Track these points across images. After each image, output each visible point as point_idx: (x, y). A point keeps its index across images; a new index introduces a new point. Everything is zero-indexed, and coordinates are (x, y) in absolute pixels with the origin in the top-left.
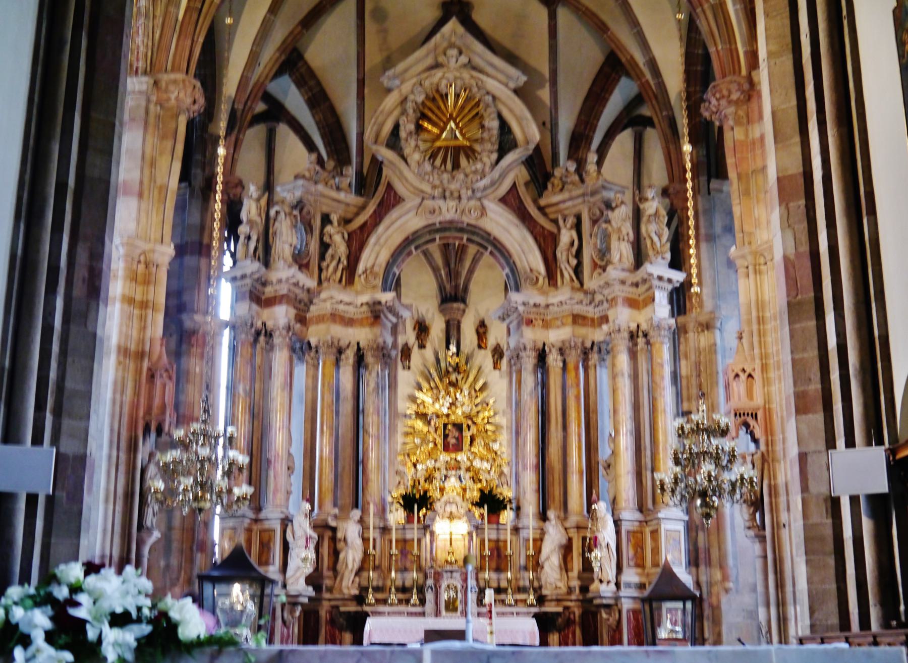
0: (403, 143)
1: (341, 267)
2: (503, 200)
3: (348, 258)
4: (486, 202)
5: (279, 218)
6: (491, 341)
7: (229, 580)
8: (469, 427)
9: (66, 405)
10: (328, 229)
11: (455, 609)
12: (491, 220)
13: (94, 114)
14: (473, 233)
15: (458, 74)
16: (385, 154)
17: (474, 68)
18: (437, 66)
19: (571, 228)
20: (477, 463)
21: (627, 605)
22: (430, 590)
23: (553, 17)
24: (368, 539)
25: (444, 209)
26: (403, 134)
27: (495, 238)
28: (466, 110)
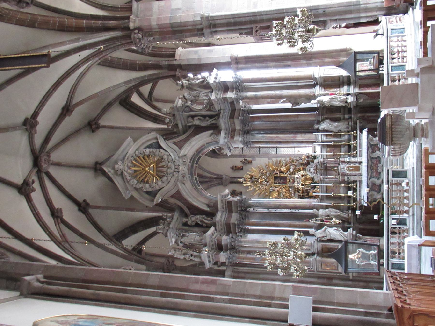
0: (154, 190)
1: (206, 218)
2: (180, 148)
3: (202, 215)
4: (181, 154)
5: (184, 242)
8: (276, 174)
9: (269, 295)
10: (189, 223)
11: (359, 167)
12: (188, 153)
13: (129, 282)
14: (194, 161)
15: (126, 165)
17: (124, 159)
19: (193, 119)
20: (291, 170)
21: (357, 91)
22: (349, 178)
23: (104, 127)
24: (326, 205)
25: (183, 172)
26: (150, 190)
27: (196, 152)
28: (142, 163)
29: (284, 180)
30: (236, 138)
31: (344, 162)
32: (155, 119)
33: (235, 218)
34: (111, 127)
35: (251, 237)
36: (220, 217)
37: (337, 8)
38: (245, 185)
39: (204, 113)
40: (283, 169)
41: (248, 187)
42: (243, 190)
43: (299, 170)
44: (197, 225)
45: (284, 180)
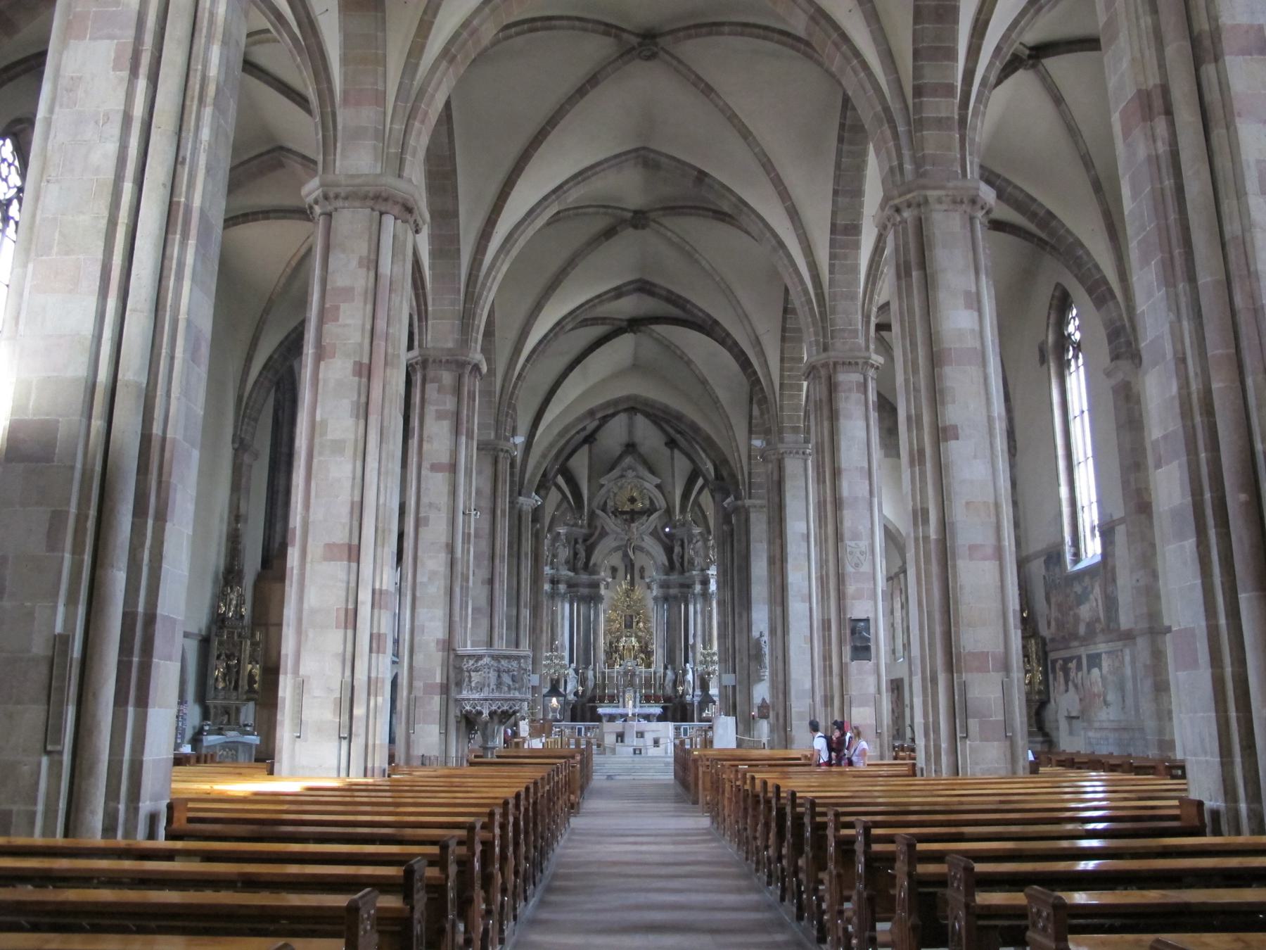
2: (651, 534)
6: (647, 574)
10: (578, 546)
16: (599, 512)
18: (622, 476)
20: (640, 634)
21: (696, 704)
29: (629, 625)
30: (661, 590)
31: (635, 692)
32: (686, 496)
33: (584, 591)
34: (672, 459)
35: (567, 606)
36: (584, 577)
37: (817, 681)
40: (641, 625)
41: (621, 585)
42: (617, 580)
43: (639, 642)
44: (576, 554)
45: (629, 625)
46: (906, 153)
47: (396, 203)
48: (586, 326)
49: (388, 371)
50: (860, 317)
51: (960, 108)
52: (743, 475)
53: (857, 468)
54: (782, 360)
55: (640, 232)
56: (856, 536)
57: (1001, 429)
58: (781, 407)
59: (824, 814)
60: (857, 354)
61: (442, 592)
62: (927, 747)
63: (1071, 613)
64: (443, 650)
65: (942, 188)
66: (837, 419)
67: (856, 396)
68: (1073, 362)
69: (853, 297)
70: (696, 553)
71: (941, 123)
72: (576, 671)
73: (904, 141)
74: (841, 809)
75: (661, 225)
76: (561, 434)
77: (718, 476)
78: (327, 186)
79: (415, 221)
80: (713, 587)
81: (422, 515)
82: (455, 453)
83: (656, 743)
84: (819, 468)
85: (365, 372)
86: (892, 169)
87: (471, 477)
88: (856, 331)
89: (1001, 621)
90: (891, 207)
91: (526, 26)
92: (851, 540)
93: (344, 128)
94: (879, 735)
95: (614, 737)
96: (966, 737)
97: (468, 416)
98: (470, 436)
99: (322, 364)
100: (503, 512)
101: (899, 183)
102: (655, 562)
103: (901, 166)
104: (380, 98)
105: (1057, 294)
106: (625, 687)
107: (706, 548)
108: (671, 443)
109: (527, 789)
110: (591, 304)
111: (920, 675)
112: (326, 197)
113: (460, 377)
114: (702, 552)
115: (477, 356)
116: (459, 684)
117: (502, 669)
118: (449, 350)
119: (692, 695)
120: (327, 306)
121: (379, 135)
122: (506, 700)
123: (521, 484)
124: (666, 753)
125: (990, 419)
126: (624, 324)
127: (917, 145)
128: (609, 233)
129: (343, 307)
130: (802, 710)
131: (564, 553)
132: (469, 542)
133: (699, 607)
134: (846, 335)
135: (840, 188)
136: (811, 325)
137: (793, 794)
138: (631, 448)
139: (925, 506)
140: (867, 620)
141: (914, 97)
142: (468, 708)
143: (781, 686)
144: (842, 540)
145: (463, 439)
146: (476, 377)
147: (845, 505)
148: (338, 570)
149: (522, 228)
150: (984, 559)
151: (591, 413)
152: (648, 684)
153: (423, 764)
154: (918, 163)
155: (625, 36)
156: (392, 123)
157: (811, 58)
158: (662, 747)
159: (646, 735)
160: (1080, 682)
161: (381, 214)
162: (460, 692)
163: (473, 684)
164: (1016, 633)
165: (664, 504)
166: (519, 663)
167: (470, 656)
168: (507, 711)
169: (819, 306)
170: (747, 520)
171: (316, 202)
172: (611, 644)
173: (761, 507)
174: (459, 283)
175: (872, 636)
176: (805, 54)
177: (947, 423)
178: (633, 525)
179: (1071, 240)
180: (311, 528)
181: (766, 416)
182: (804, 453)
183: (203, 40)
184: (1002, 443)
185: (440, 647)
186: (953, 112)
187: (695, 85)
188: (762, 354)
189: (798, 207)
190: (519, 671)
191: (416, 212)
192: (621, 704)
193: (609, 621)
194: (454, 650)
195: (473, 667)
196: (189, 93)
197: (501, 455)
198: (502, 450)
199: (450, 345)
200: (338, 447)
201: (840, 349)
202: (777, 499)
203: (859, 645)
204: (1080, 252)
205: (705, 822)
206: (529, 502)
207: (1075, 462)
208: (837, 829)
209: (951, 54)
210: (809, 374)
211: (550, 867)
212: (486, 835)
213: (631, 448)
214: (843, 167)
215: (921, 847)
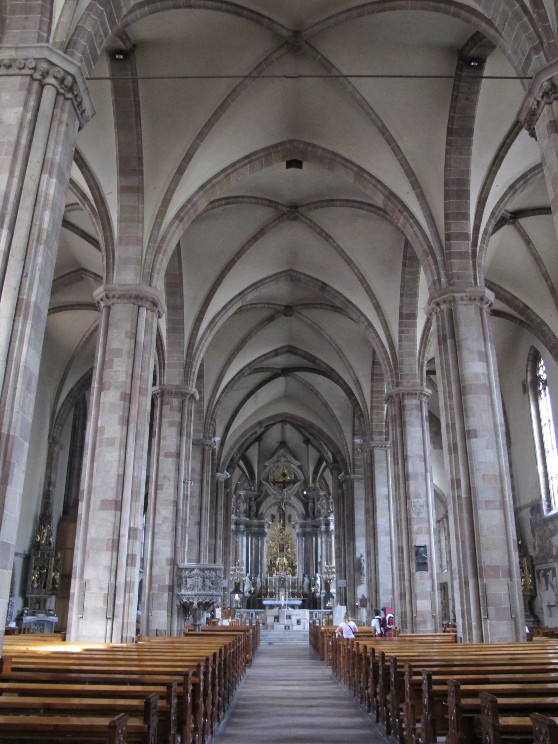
2: (295, 495)
6: (293, 519)
7: (235, 593)
10: (252, 502)
20: (288, 555)
21: (322, 598)
30: (301, 529)
31: (286, 591)
32: (316, 472)
33: (255, 529)
35: (245, 539)
36: (255, 521)
37: (395, 584)
38: (278, 525)
39: (316, 509)
40: (289, 550)
41: (277, 526)
43: (288, 560)
46: (442, 272)
47: (147, 300)
48: (258, 372)
49: (141, 398)
50: (417, 367)
51: (472, 246)
52: (349, 460)
53: (417, 455)
54: (372, 392)
55: (289, 318)
56: (418, 496)
57: (502, 432)
58: (372, 419)
59: (402, 667)
60: (416, 388)
61: (170, 529)
62: (463, 625)
63: (548, 541)
64: (171, 565)
65: (463, 291)
66: (405, 427)
67: (416, 413)
68: (542, 392)
69: (413, 355)
70: (322, 507)
71: (462, 255)
72: (250, 578)
73: (440, 265)
74: (413, 664)
75: (301, 314)
76: (242, 436)
77: (335, 461)
78: (108, 291)
79: (158, 311)
80: (332, 527)
81: (159, 483)
82: (179, 446)
83: (298, 622)
84: (395, 455)
85: (128, 399)
86: (434, 281)
87: (189, 461)
88: (415, 375)
89: (506, 547)
90: (434, 303)
91: (224, 202)
92: (415, 498)
93: (119, 257)
94: (434, 617)
95: (273, 619)
96: (487, 619)
97: (187, 425)
98: (188, 436)
99: (103, 393)
100: (207, 481)
101: (438, 289)
102: (297, 512)
103: (439, 279)
104: (140, 241)
105: (532, 352)
106: (280, 588)
107: (328, 503)
108: (307, 441)
109: (220, 650)
110: (260, 360)
111: (458, 580)
112: (107, 297)
113: (183, 402)
114: (325, 507)
115: (193, 390)
116: (180, 586)
117: (206, 576)
118: (177, 386)
119: (321, 593)
120: (106, 359)
121: (139, 262)
122: (208, 595)
123: (218, 465)
124: (305, 628)
125: (495, 425)
126: (279, 371)
127: (447, 267)
128: (271, 319)
129: (115, 360)
130: (387, 601)
131: (243, 507)
132: (187, 500)
133: (324, 539)
134: (409, 377)
135: (405, 292)
136: (388, 371)
137: (383, 654)
138: (283, 444)
139: (458, 477)
140: (425, 547)
141: (446, 240)
142: (185, 600)
143: (374, 587)
144: (409, 498)
145: (184, 438)
146: (192, 402)
147: (411, 478)
148: (109, 515)
149: (220, 315)
150: (495, 509)
151: (260, 423)
152: (293, 586)
153: (157, 635)
154: (449, 277)
155: (280, 206)
156: (146, 255)
157: (386, 219)
158: (302, 625)
159: (293, 617)
160: (555, 584)
161: (139, 307)
162: (180, 591)
163: (188, 586)
164: (515, 555)
165: (302, 477)
166: (216, 573)
167: (186, 569)
168: (208, 602)
169: (393, 360)
170: (352, 487)
171: (102, 300)
172: (271, 561)
173: (360, 479)
174: (183, 347)
175: (428, 557)
176: (382, 216)
177: (470, 428)
178: (284, 490)
179: (538, 321)
180: (93, 490)
181: (363, 425)
182: (385, 447)
183: (41, 208)
184: (502, 439)
185: (169, 563)
186: (468, 249)
187: (319, 233)
188: (360, 388)
189: (380, 303)
190: (216, 578)
191: (159, 306)
192: (277, 598)
193: (270, 547)
194: (177, 565)
195: (188, 576)
196: (31, 237)
197: (207, 448)
198: (207, 445)
199: (178, 383)
200: (110, 442)
201: (406, 386)
202: (369, 474)
203: (420, 561)
204: (545, 328)
205: (329, 671)
206: (223, 476)
207: (546, 451)
208: (410, 676)
209: (466, 216)
210: (388, 400)
211: (234, 701)
212: (195, 679)
213: (283, 444)
214: (405, 280)
215: (463, 687)
